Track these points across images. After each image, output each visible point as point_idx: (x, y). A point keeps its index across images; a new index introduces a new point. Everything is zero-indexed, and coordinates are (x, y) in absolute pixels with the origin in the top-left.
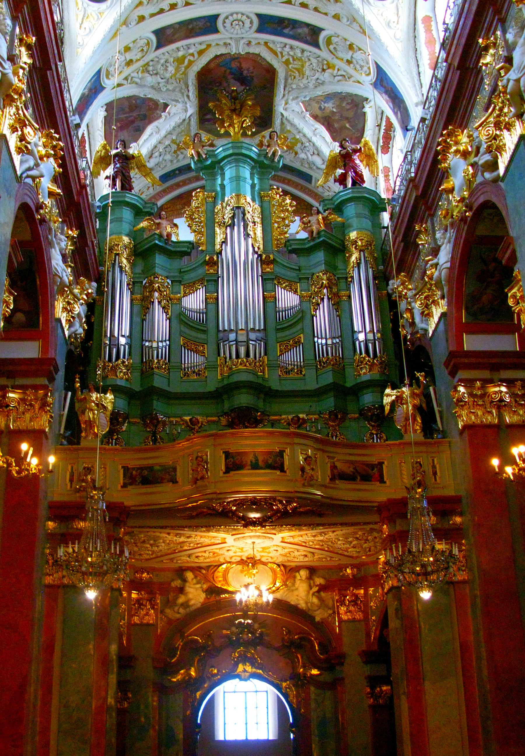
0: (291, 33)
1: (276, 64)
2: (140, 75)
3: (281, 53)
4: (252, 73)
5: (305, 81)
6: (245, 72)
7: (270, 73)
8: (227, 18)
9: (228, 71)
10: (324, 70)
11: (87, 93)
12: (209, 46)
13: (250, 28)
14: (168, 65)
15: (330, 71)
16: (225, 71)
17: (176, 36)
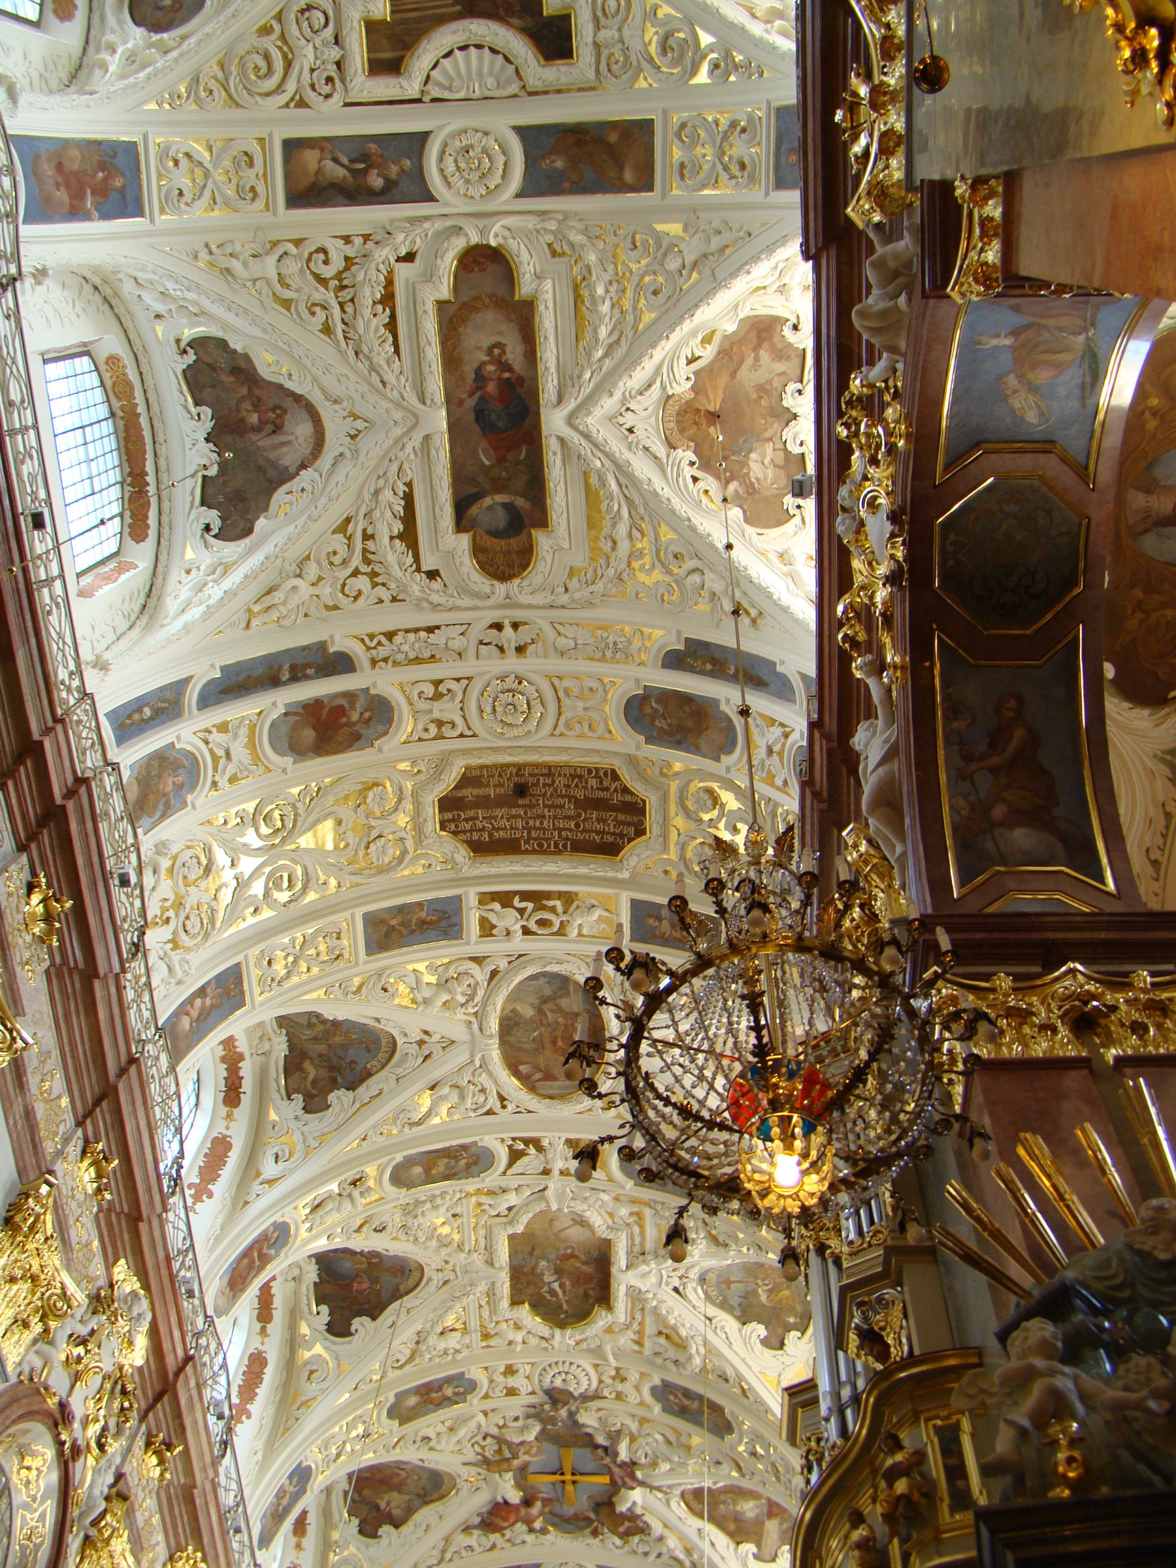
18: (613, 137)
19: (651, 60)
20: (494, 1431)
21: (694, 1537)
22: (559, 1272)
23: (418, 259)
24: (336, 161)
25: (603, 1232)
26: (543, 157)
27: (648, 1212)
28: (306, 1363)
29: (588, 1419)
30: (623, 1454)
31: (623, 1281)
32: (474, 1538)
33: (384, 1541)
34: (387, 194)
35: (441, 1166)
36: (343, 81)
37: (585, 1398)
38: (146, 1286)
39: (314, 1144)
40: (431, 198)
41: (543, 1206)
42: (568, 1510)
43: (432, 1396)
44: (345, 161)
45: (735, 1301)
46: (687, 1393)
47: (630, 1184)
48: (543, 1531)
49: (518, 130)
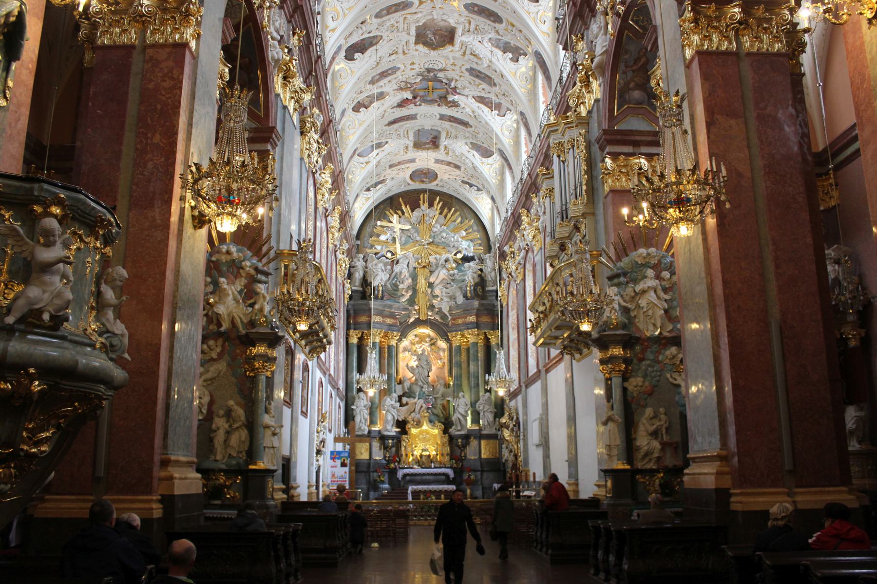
20: (405, 80)
21: (476, 109)
22: (434, 34)
25: (454, 25)
27: (472, 21)
28: (338, 71)
29: (441, 75)
30: (453, 85)
31: (459, 39)
32: (394, 110)
33: (362, 113)
35: (393, 9)
37: (440, 70)
38: (321, 110)
39: (347, 12)
41: (430, 17)
42: (429, 99)
43: (383, 75)
45: (502, 45)
46: (479, 72)
47: (466, 13)
48: (420, 105)
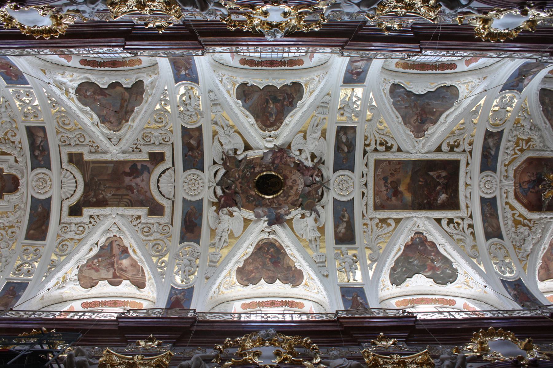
0: (494, 150)
1: (524, 158)
2: (522, 251)
3: (513, 155)
4: (533, 173)
5: (535, 137)
6: (532, 178)
7: (530, 161)
8: (483, 192)
9: (531, 190)
10: (523, 126)
11: (516, 292)
12: (507, 203)
13: (491, 176)
14: (518, 231)
15: (521, 122)
16: (531, 192)
17: (495, 225)
18: (44, 228)
19: (63, 241)
23: (16, 164)
24: (42, 141)
26: (42, 205)
34: (33, 157)
36: (65, 145)
40: (32, 169)
44: (42, 144)
49: (50, 199)
